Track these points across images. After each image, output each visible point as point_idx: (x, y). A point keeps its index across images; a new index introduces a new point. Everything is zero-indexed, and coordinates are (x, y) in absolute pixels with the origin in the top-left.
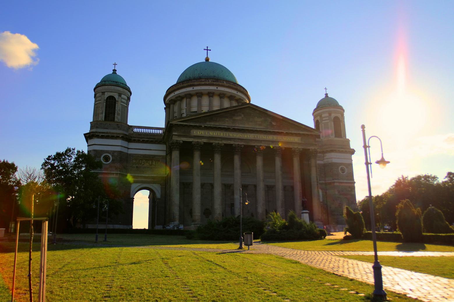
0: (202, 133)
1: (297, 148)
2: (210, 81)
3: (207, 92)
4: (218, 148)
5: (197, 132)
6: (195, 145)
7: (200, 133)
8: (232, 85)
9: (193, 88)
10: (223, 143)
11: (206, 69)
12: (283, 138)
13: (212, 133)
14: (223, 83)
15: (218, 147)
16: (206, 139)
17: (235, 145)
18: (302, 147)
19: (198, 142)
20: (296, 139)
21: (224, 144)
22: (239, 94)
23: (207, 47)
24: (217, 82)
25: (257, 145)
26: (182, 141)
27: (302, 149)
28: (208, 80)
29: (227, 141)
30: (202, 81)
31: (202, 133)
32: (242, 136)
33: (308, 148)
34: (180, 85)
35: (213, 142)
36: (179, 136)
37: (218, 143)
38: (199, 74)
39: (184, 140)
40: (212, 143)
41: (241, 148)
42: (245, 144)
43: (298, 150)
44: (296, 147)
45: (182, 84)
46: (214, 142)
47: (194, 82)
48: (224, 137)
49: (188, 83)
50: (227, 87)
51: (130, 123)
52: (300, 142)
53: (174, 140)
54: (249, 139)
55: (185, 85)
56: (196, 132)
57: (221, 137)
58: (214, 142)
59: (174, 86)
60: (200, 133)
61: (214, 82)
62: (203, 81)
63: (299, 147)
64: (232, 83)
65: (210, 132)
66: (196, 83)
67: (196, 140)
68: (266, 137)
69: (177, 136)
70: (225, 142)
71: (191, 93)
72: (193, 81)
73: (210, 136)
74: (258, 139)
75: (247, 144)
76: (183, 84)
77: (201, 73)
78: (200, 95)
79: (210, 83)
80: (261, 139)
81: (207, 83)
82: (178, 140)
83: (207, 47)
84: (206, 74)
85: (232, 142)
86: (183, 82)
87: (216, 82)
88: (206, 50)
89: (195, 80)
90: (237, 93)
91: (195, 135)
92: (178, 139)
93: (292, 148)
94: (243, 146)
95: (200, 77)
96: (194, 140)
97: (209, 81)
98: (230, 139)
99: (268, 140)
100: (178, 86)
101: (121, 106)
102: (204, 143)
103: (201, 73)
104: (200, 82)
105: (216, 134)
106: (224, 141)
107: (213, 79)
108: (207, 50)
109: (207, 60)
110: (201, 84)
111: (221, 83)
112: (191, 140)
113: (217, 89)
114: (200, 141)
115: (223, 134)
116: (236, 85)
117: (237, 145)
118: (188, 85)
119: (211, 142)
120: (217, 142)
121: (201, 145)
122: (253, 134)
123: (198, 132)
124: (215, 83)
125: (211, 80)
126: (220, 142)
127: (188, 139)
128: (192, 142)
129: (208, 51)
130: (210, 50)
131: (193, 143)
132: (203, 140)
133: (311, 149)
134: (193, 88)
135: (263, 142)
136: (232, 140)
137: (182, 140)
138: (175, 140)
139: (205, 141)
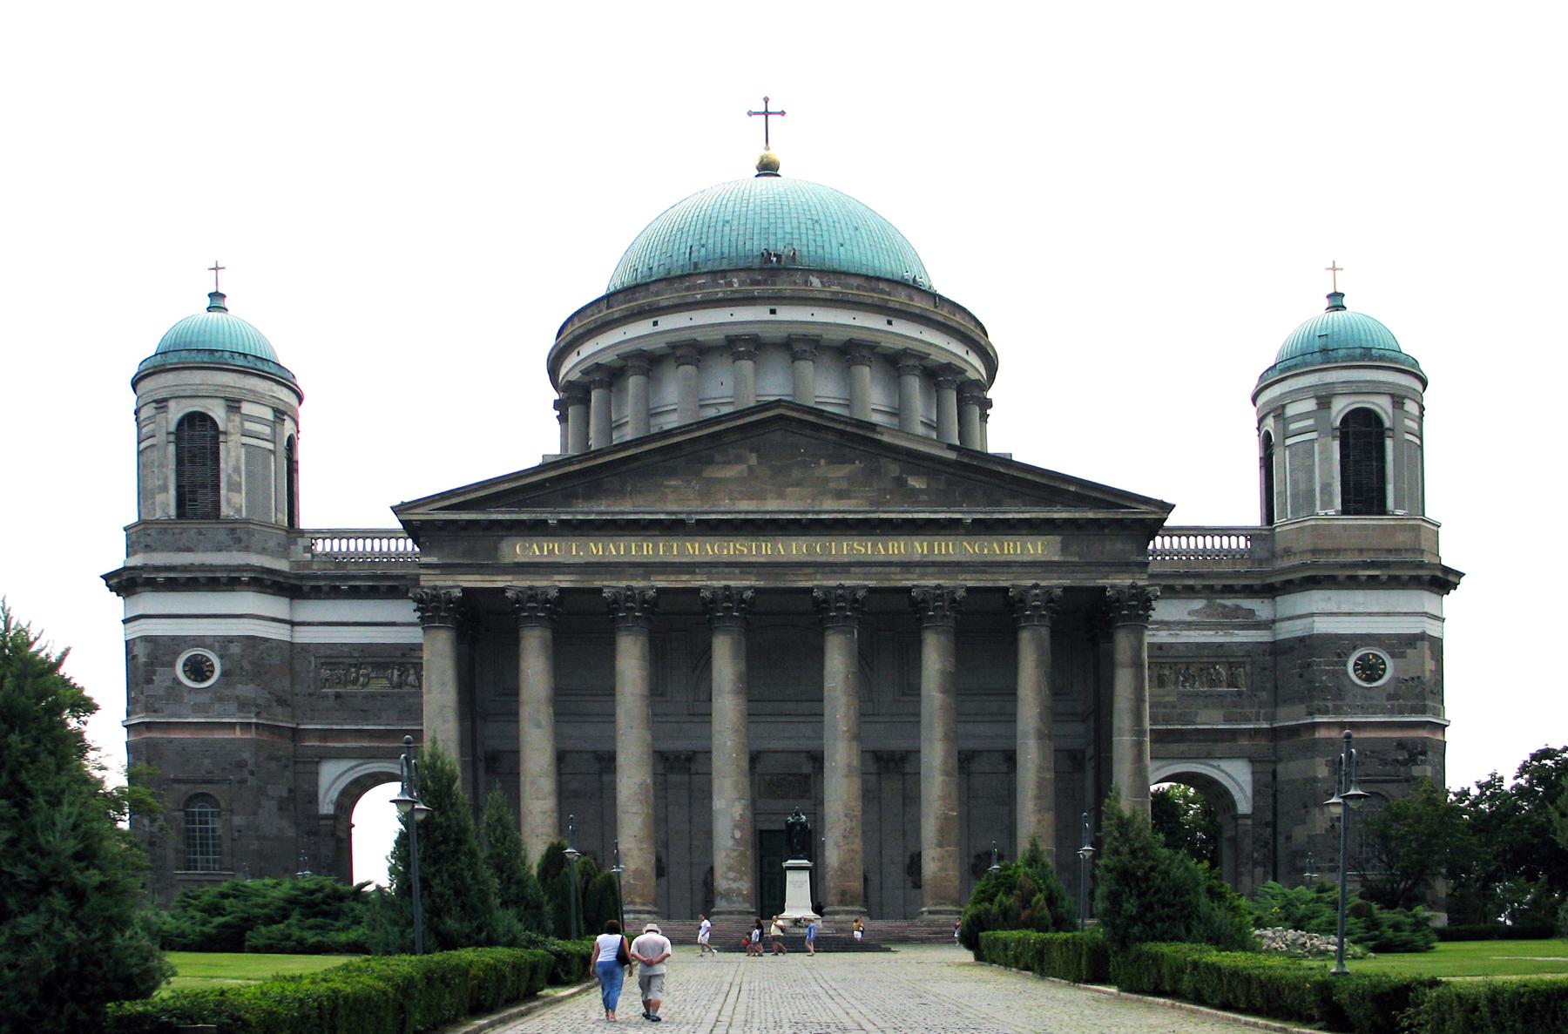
0: (551, 552)
1: (1036, 586)
2: (735, 280)
3: (723, 337)
4: (628, 608)
5: (531, 546)
6: (517, 601)
7: (541, 550)
8: (858, 288)
9: (655, 324)
10: (652, 588)
11: (728, 222)
12: (965, 543)
13: (600, 545)
14: (806, 282)
15: (629, 605)
16: (572, 573)
17: (714, 590)
18: (1067, 582)
19: (531, 588)
20: (1036, 548)
21: (657, 589)
22: (902, 328)
23: (766, 100)
24: (774, 283)
25: (819, 587)
26: (459, 590)
27: (1058, 592)
28: (725, 278)
29: (673, 578)
30: (694, 287)
31: (551, 552)
32: (750, 549)
33: (1100, 582)
34: (600, 311)
35: (605, 583)
36: (446, 568)
37: (629, 588)
38: (691, 247)
39: (466, 585)
40: (599, 591)
41: (743, 601)
42: (761, 584)
43: (1037, 595)
44: (1030, 583)
45: (608, 308)
46: (610, 584)
47: (657, 293)
48: (658, 560)
49: (629, 302)
50: (826, 300)
51: (308, 519)
52: (1056, 558)
53: (423, 587)
54: (785, 560)
55: (617, 310)
56: (523, 548)
57: (645, 560)
58: (608, 587)
59: (576, 319)
60: (541, 550)
61: (755, 283)
62: (702, 286)
63: (1043, 583)
64: (855, 282)
65: (592, 545)
66: (665, 299)
67: (523, 582)
68: (874, 546)
69: (438, 572)
70: (661, 582)
71: (647, 346)
72: (653, 288)
73: (596, 560)
74: (831, 559)
75: (771, 584)
76: (612, 307)
77: (703, 246)
78: (693, 352)
79: (732, 292)
80: (846, 560)
81: (720, 295)
82: (441, 588)
83: (766, 100)
84: (726, 251)
85: (698, 577)
86: (612, 300)
87: (765, 282)
88: (756, 113)
89: (664, 283)
90: (890, 323)
91: (516, 560)
92: (438, 583)
93: (1006, 589)
94: (749, 593)
95: (696, 264)
96: (515, 583)
97: (730, 284)
98: (690, 568)
99: (881, 559)
100: (593, 315)
101: (243, 450)
102: (561, 590)
103: (703, 246)
104: (688, 289)
105: (618, 550)
106: (659, 578)
107: (749, 269)
108: (767, 113)
109: (768, 168)
110: (690, 300)
111: (795, 283)
112: (499, 582)
113: (772, 317)
114: (541, 583)
115: (656, 548)
116: (882, 285)
117: (720, 592)
118: (627, 309)
119: (597, 584)
120: (623, 584)
121: (548, 601)
122: (803, 538)
123: (535, 546)
124: (757, 290)
125: (743, 275)
126: (638, 584)
127: (487, 578)
128: (503, 590)
129: (769, 117)
130: (783, 113)
131: (509, 594)
132: (556, 577)
133: (1112, 587)
134: (655, 324)
135: (852, 569)
136: (697, 570)
137: (458, 586)
138: (428, 587)
139: (565, 581)
